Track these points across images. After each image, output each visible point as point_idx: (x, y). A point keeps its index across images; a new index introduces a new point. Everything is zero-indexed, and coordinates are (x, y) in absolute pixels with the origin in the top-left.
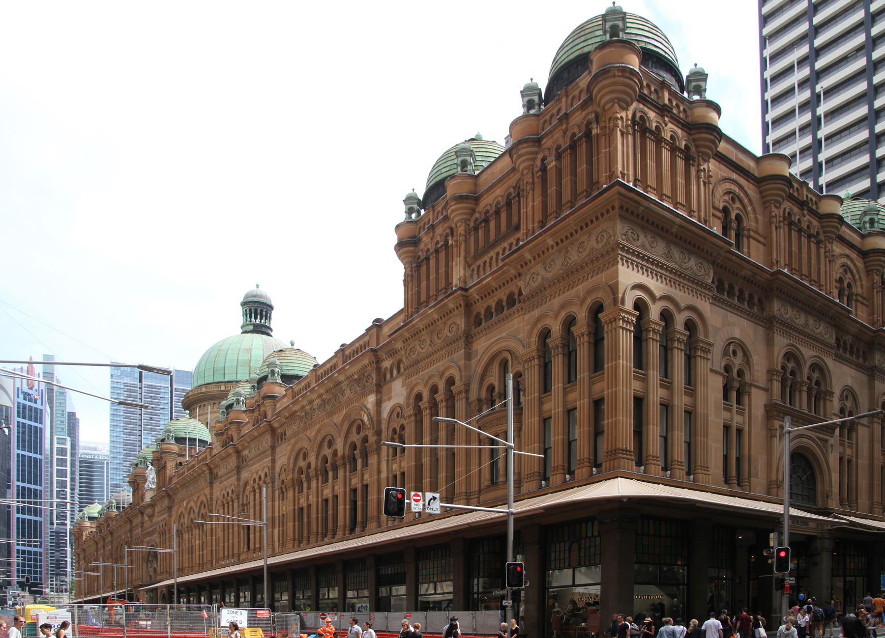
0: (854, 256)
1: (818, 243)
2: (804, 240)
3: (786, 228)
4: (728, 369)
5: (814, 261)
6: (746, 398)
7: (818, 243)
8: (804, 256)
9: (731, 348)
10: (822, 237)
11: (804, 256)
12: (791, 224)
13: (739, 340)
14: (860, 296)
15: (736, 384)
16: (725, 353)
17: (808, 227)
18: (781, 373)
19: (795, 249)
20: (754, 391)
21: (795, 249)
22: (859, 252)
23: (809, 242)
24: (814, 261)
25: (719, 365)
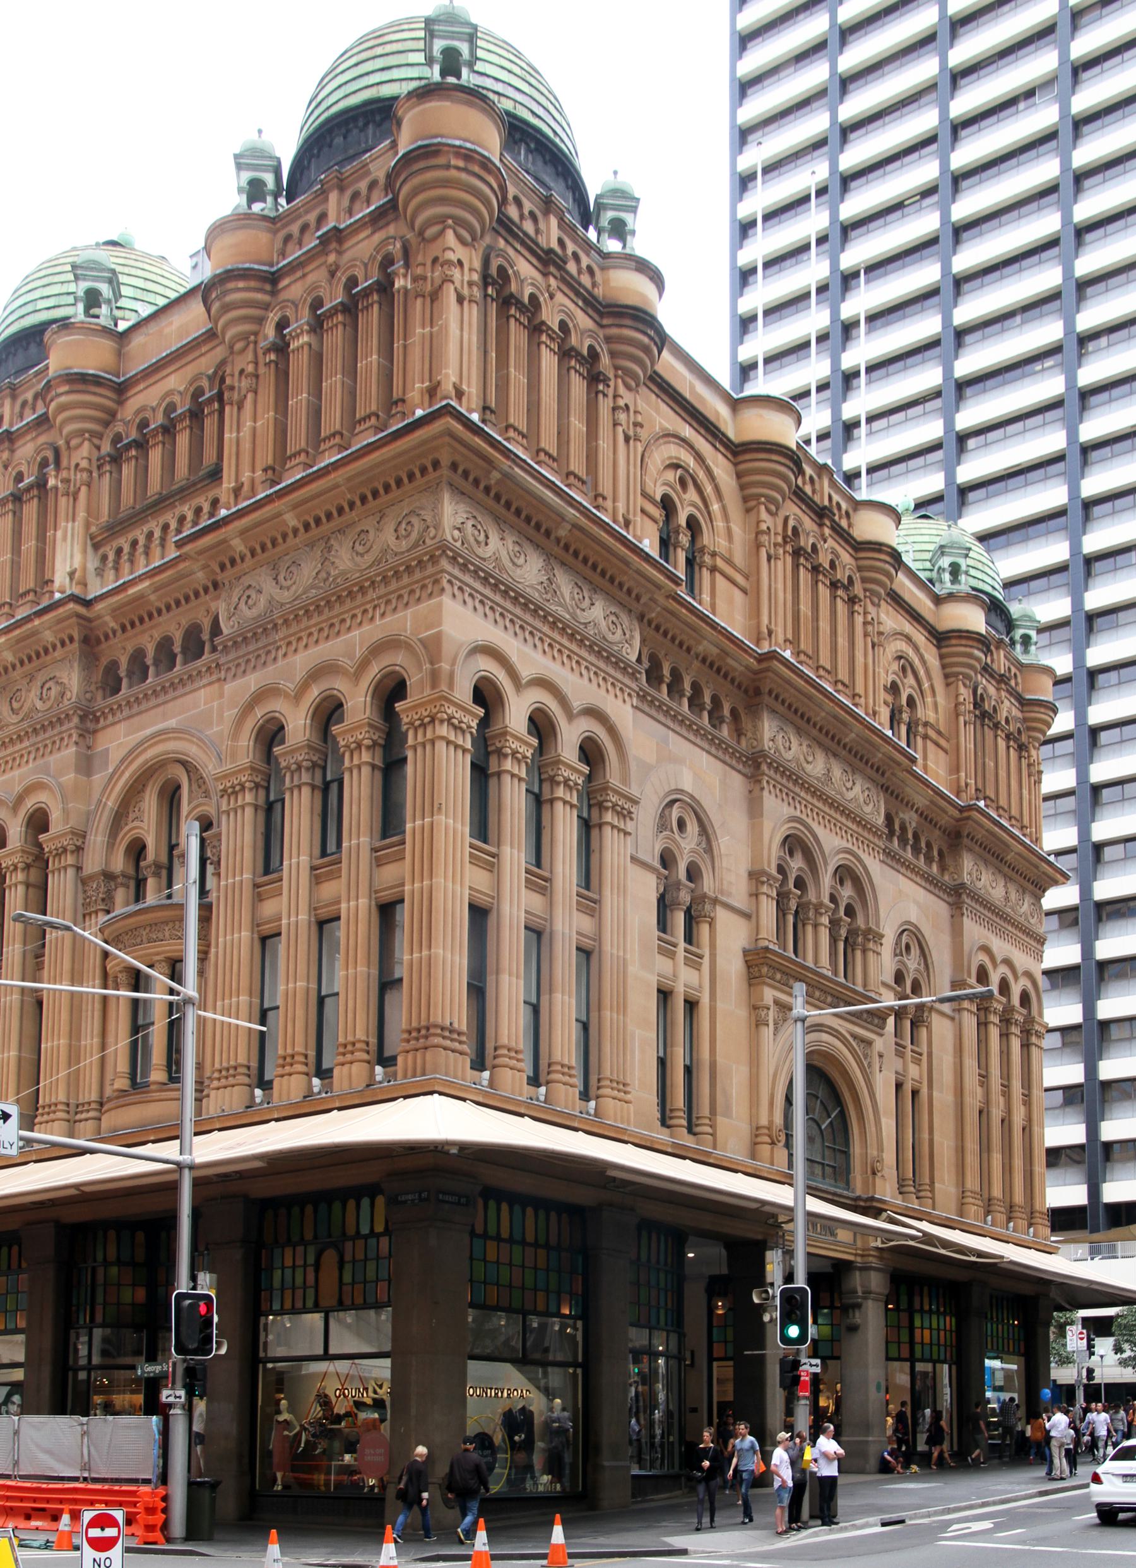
0: (920, 638)
1: (852, 601)
2: (824, 592)
3: (789, 559)
4: (667, 859)
5: (842, 641)
6: (705, 929)
7: (852, 601)
8: (824, 625)
9: (675, 813)
10: (858, 589)
11: (824, 625)
12: (797, 553)
13: (692, 797)
14: (932, 727)
15: (685, 897)
16: (662, 824)
17: (832, 564)
18: (774, 878)
19: (805, 608)
20: (721, 914)
21: (805, 608)
22: (930, 633)
23: (834, 597)
24: (842, 641)
25: (651, 848)
